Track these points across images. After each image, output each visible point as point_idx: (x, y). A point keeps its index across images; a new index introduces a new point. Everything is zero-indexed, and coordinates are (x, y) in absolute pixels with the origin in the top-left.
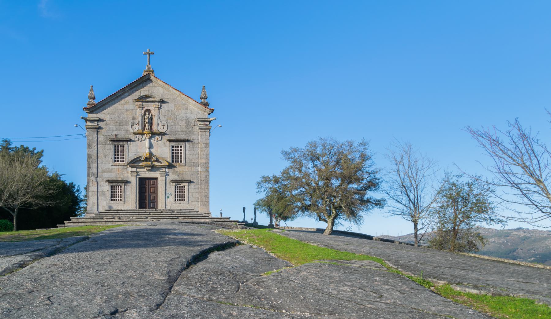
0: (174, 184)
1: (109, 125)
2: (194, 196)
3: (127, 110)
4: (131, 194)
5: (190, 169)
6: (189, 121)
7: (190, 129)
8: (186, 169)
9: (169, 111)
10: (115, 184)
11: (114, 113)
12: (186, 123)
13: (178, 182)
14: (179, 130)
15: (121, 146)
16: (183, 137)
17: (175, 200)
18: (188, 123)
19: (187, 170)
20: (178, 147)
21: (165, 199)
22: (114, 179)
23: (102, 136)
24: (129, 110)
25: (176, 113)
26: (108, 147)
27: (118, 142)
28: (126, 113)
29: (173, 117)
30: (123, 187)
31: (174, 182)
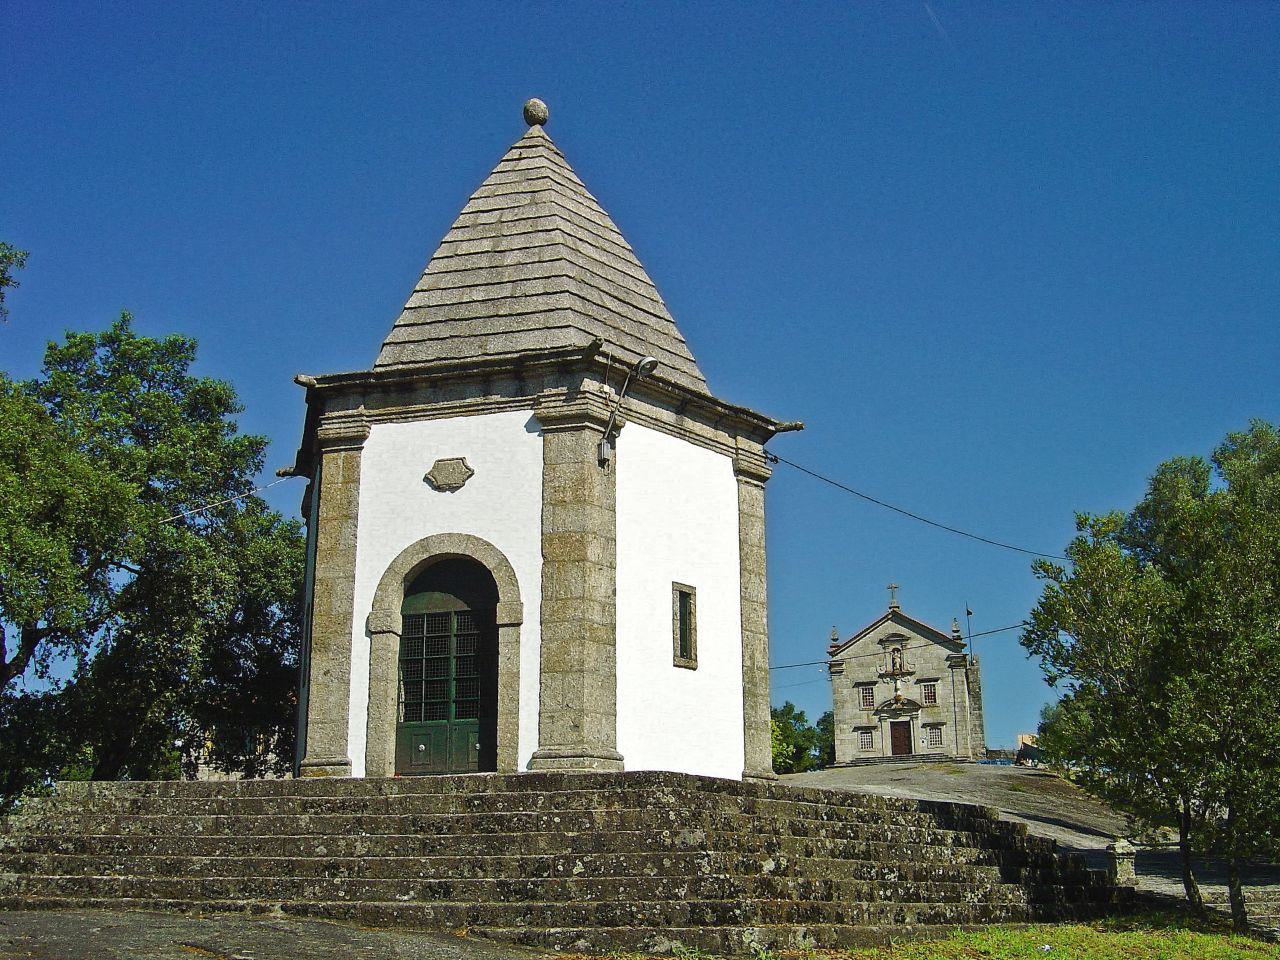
21: (921, 742)
27: (867, 686)
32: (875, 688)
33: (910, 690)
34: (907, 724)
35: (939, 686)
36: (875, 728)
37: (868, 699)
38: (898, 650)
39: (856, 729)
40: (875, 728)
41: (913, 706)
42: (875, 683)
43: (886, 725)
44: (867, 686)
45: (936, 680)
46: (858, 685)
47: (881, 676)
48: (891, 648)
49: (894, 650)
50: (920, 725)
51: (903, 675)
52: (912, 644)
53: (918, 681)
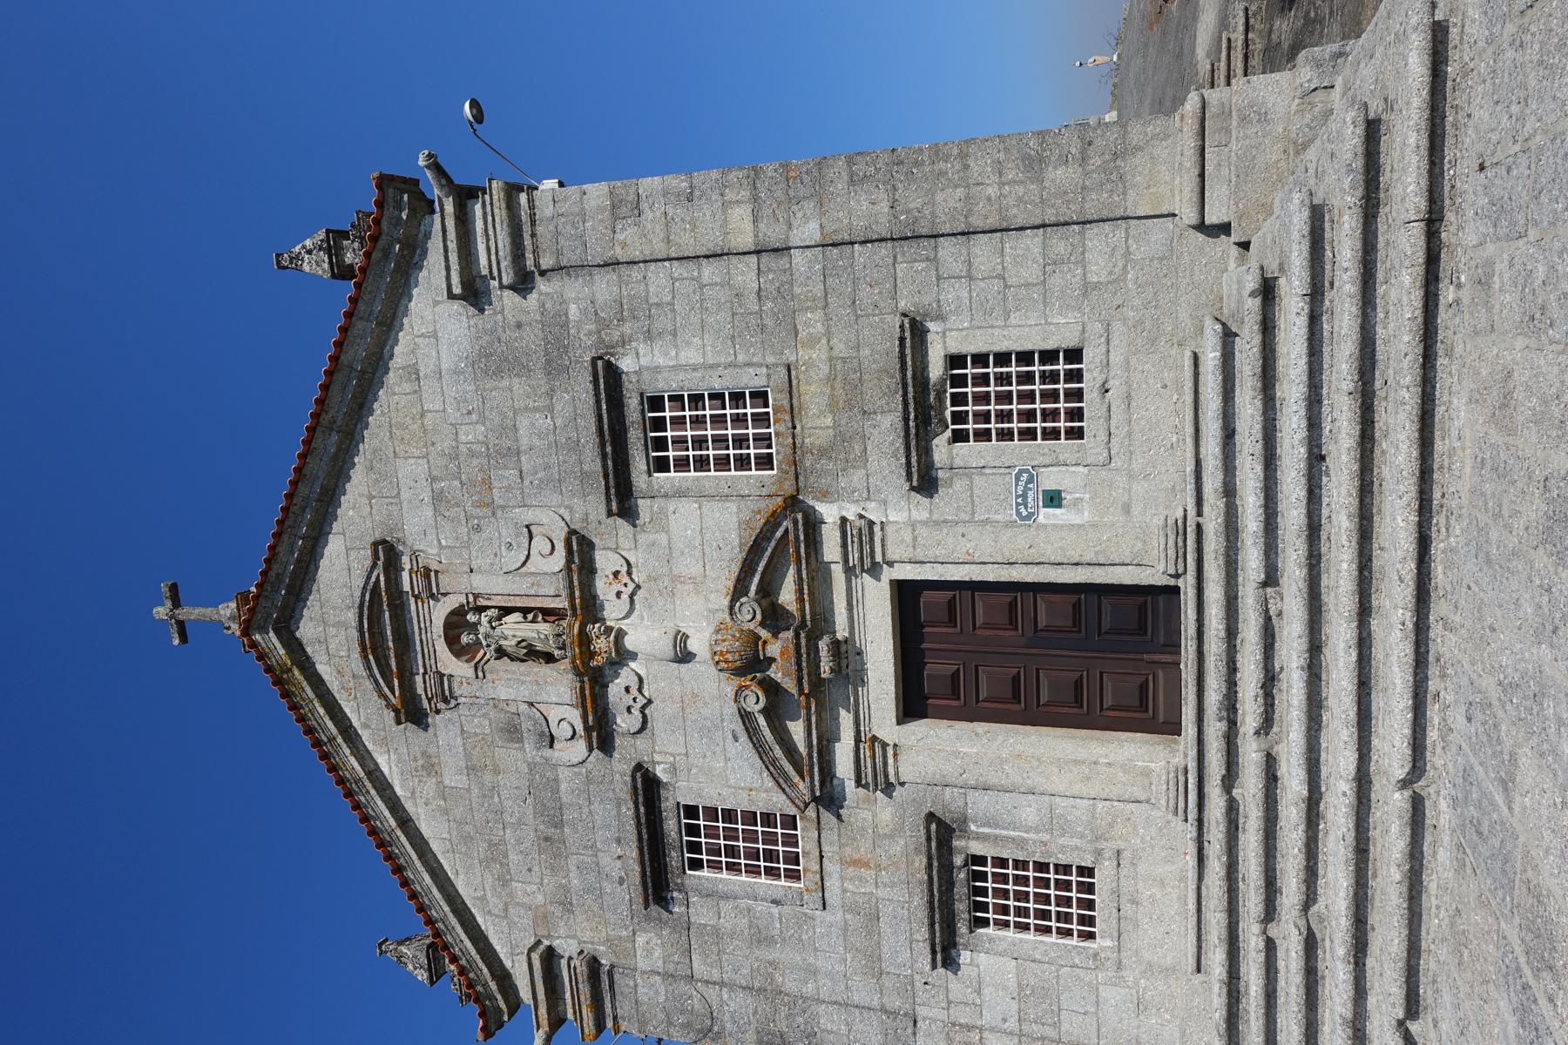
0: (941, 449)
1: (566, 889)
2: (1031, 272)
3: (471, 770)
4: (1036, 781)
5: (811, 323)
6: (485, 354)
7: (531, 338)
8: (814, 360)
9: (438, 499)
10: (961, 907)
11: (496, 854)
12: (498, 373)
13: (922, 416)
14: (544, 423)
15: (693, 830)
16: (578, 397)
17: (1076, 434)
18: (491, 362)
19: (818, 354)
20: (659, 424)
22: (919, 901)
23: (641, 940)
24: (468, 756)
25: (446, 444)
26: (701, 913)
27: (665, 847)
28: (488, 778)
29: (471, 469)
30: (976, 848)
31: (925, 452)
32: (682, 790)
33: (680, 570)
34: (906, 595)
35: (649, 364)
36: (941, 832)
37: (763, 845)
38: (456, 624)
39: (945, 952)
40: (941, 832)
41: (782, 546)
42: (647, 788)
43: (939, 752)
44: (665, 847)
45: (609, 380)
46: (657, 886)
47: (601, 733)
48: (448, 662)
49: (458, 650)
50: (920, 508)
51: (589, 608)
52: (426, 537)
53: (623, 501)
